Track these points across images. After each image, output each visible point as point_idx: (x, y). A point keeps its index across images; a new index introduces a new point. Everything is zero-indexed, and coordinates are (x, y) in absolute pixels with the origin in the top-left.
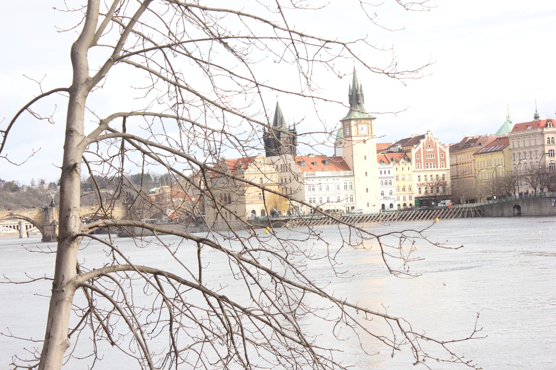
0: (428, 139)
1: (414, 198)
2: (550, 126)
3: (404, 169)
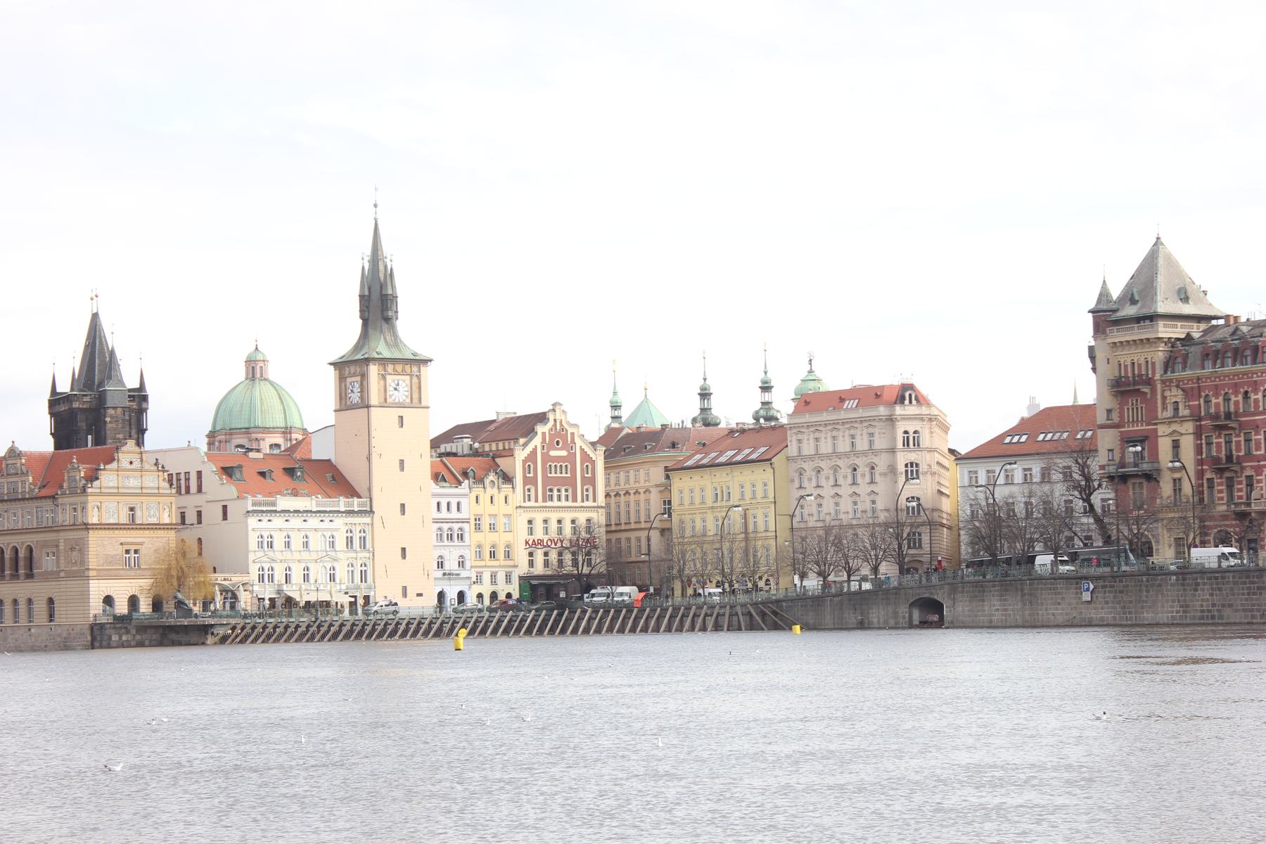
0: (555, 425)
1: (517, 579)
2: (910, 402)
3: (495, 499)
